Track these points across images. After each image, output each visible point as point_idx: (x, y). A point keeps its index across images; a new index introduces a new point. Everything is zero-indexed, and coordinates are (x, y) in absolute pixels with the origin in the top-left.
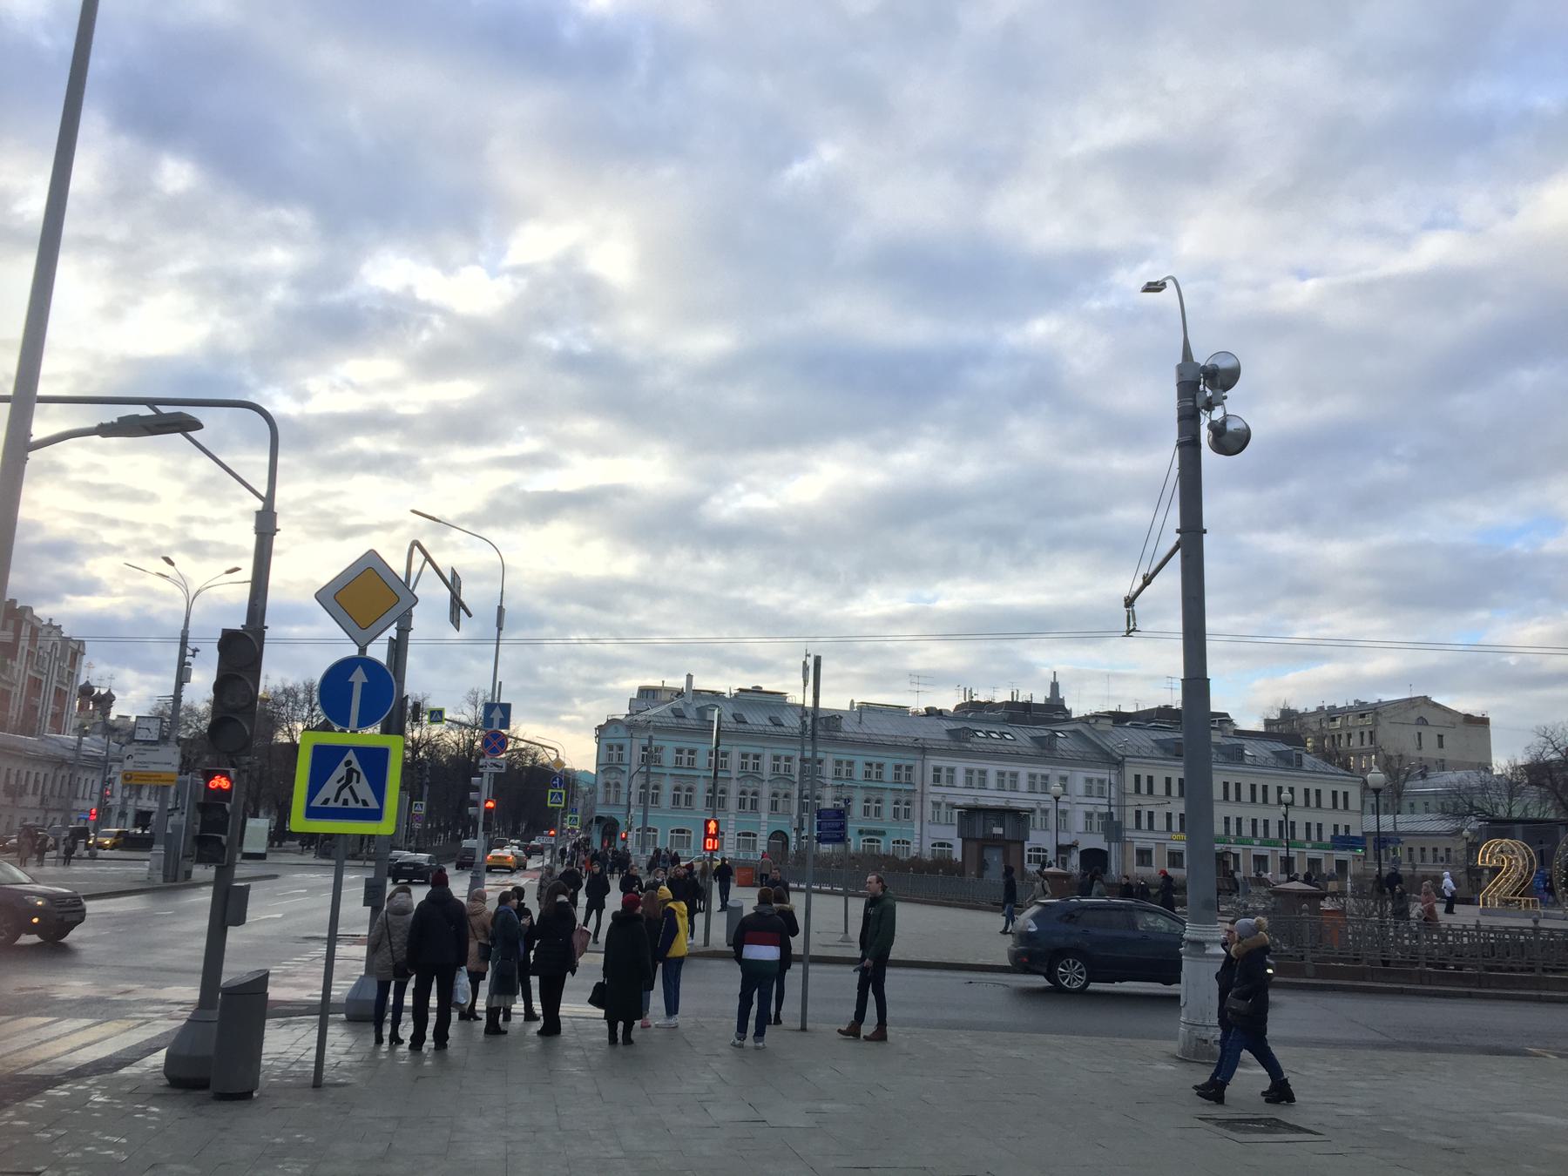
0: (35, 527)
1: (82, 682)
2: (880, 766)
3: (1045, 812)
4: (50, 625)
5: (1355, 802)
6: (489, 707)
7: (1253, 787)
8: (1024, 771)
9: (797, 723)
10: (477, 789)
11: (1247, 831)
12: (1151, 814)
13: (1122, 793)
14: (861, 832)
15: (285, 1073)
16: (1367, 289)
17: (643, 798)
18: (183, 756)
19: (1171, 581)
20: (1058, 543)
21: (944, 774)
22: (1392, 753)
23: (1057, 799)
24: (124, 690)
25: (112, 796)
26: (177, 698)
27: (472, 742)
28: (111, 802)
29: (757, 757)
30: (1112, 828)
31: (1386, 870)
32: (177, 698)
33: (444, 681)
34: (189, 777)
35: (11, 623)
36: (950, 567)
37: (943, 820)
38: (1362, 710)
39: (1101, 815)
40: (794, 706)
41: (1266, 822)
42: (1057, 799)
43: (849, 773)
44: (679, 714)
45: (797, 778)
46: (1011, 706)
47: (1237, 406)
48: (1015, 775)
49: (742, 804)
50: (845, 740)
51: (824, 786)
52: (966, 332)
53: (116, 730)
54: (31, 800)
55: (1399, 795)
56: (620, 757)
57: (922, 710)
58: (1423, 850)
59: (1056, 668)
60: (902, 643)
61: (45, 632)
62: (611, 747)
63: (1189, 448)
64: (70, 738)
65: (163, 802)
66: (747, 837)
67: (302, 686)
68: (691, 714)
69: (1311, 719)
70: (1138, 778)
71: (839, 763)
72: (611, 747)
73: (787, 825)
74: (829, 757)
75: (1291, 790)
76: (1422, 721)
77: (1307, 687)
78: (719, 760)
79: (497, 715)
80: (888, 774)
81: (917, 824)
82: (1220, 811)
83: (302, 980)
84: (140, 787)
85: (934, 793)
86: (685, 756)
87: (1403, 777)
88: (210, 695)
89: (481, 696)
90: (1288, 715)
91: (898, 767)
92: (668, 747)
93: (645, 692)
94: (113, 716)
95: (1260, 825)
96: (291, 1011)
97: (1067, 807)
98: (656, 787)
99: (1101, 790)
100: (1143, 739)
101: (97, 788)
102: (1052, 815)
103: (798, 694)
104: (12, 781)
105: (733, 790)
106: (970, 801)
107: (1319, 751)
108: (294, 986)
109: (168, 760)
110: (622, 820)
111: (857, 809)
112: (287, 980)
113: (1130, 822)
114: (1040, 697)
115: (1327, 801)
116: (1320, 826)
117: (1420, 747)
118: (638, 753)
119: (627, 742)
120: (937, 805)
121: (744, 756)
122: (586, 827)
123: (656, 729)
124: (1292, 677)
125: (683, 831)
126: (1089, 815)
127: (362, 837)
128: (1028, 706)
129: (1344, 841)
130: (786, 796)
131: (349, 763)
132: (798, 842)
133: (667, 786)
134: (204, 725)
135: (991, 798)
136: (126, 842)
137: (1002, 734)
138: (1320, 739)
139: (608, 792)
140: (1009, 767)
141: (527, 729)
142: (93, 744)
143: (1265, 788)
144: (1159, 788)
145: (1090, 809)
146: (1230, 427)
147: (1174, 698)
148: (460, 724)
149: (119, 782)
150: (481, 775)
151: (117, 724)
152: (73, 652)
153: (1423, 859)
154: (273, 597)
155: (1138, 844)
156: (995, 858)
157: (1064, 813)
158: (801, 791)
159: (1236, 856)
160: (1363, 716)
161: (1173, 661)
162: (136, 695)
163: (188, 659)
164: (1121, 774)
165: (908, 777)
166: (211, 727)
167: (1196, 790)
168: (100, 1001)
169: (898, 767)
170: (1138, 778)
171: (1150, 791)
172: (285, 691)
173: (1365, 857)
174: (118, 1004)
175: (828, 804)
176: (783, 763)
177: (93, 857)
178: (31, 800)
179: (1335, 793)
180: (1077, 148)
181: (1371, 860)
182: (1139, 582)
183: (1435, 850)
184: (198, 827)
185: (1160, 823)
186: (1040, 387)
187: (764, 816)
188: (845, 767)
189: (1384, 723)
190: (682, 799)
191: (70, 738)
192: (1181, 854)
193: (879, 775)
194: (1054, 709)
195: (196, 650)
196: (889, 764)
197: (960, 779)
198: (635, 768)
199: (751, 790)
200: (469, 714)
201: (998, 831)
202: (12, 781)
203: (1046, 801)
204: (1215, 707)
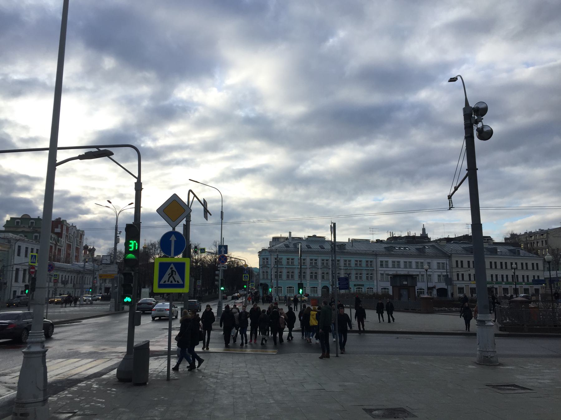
1: (84, 245)
2: (360, 261)
3: (423, 275)
4: (72, 226)
5: (541, 266)
6: (220, 247)
7: (501, 263)
8: (414, 261)
9: (330, 247)
10: (218, 275)
11: (500, 279)
12: (463, 275)
13: (451, 268)
14: (355, 285)
15: (158, 376)
16: (552, 69)
17: (276, 276)
18: (119, 268)
19: (465, 189)
20: (429, 176)
21: (384, 263)
22: (554, 248)
23: (427, 270)
24: (99, 246)
26: (115, 248)
27: (216, 259)
28: (96, 285)
29: (316, 260)
30: (448, 280)
31: (554, 291)
32: (115, 248)
33: (204, 238)
36: (389, 187)
37: (385, 280)
38: (542, 233)
39: (444, 276)
40: (328, 241)
41: (507, 276)
42: (427, 270)
43: (349, 264)
44: (287, 246)
45: (331, 267)
46: (408, 237)
47: (488, 122)
48: (410, 262)
49: (311, 277)
50: (347, 253)
51: (341, 269)
52: (397, 98)
53: (96, 260)
54: (70, 285)
56: (267, 262)
57: (375, 240)
59: (424, 223)
60: (368, 217)
62: (264, 259)
63: (469, 139)
65: (113, 285)
66: (314, 289)
67: (157, 243)
68: (291, 246)
69: (523, 237)
70: (457, 261)
71: (345, 261)
72: (264, 259)
73: (328, 284)
74: (342, 259)
75: (516, 264)
77: (521, 225)
78: (302, 262)
79: (223, 249)
80: (364, 264)
81: (375, 282)
82: (489, 273)
83: (162, 343)
84: (105, 280)
85: (381, 270)
86: (290, 261)
89: (218, 243)
90: (513, 236)
91: (367, 262)
92: (284, 258)
93: (275, 239)
94: (95, 256)
95: (505, 277)
96: (157, 354)
97: (431, 273)
98: (281, 272)
99: (443, 267)
100: (459, 247)
101: (91, 281)
102: (425, 276)
103: (329, 237)
104: (64, 279)
105: (308, 272)
106: (395, 273)
107: (526, 248)
108: (160, 345)
109: (113, 270)
110: (269, 284)
111: (353, 277)
112: (157, 344)
113: (455, 278)
114: (418, 233)
115: (530, 267)
116: (528, 276)
118: (273, 260)
119: (269, 257)
120: (382, 274)
121: (311, 260)
122: (257, 287)
123: (279, 252)
124: (519, 221)
125: (291, 287)
126: (439, 276)
127: (179, 293)
128: (414, 237)
129: (537, 281)
130: (327, 273)
131: (172, 268)
132: (332, 290)
133: (285, 272)
135: (402, 271)
136: (104, 299)
137: (405, 248)
138: (526, 244)
139: (264, 275)
140: (408, 260)
141: (234, 254)
142: (89, 266)
143: (506, 263)
144: (465, 265)
145: (440, 274)
146: (485, 130)
147: (469, 231)
148: (211, 253)
149: (98, 279)
150: (219, 270)
152: (80, 234)
155: (458, 286)
156: (404, 292)
157: (430, 275)
158: (332, 271)
159: (496, 289)
160: (542, 235)
161: (467, 217)
162: (102, 247)
164: (450, 261)
165: (371, 265)
167: (479, 266)
169: (367, 262)
170: (457, 261)
171: (462, 266)
172: (151, 244)
173: (546, 287)
175: (342, 276)
176: (325, 262)
177: (91, 304)
178: (70, 285)
179: (533, 264)
180: (437, 24)
181: (548, 288)
182: (453, 189)
185: (466, 277)
186: (424, 117)
187: (320, 281)
188: (348, 263)
190: (290, 276)
192: (475, 289)
193: (360, 265)
194: (424, 237)
195: (120, 232)
196: (364, 260)
197: (390, 265)
198: (273, 266)
199: (314, 272)
200: (214, 250)
201: (405, 283)
202: (64, 279)
203: (423, 271)
204: (485, 234)
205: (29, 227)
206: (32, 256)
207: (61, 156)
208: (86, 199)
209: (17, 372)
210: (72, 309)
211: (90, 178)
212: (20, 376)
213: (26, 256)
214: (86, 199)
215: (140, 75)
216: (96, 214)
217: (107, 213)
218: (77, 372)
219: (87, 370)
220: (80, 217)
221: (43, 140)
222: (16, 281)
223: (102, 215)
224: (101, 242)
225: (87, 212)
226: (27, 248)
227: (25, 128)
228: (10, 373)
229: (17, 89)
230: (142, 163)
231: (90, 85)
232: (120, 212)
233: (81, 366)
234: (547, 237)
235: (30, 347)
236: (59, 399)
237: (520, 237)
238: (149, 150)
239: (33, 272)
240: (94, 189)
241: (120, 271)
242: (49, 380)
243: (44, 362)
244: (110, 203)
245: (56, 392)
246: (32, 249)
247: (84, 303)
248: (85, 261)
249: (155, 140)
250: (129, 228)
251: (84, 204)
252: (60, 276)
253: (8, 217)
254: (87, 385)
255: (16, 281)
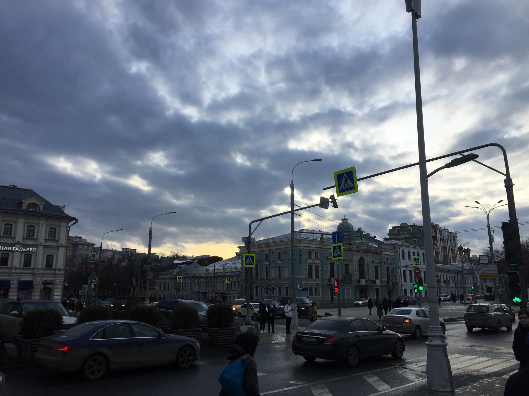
0: (436, 198)
4: (445, 229)
18: (498, 268)
25: (477, 282)
28: (478, 285)
34: (502, 275)
35: (433, 230)
61: (444, 231)
64: (459, 264)
65: (495, 284)
84: (486, 279)
88: (503, 245)
94: (471, 256)
101: (472, 280)
104: (445, 279)
109: (493, 269)
134: (503, 256)
142: (467, 266)
151: (473, 258)
152: (454, 236)
154: (516, 206)
162: (477, 248)
163: (492, 234)
166: (507, 256)
168: (490, 352)
174: (496, 353)
178: (452, 285)
184: (510, 292)
191: (459, 264)
195: (494, 231)
202: (445, 279)
205: (408, 234)
206: (415, 258)
207: (430, 167)
208: (455, 201)
209: (423, 361)
210: (458, 307)
211: (456, 181)
212: (428, 365)
213: (410, 259)
214: (455, 201)
215: (493, 64)
216: (467, 215)
217: (478, 213)
218: (476, 369)
219: (485, 368)
220: (452, 220)
221: (410, 153)
222: (405, 281)
223: (471, 216)
224: (476, 242)
225: (458, 214)
226: (409, 252)
227: (393, 147)
228: (415, 362)
229: (381, 116)
230: (508, 156)
231: (444, 92)
232: (490, 211)
233: (479, 363)
235: (431, 341)
236: (464, 392)
238: (515, 139)
239: (418, 273)
240: (461, 190)
241: (500, 271)
242: (453, 373)
243: (446, 356)
244: (478, 203)
245: (459, 386)
246: (414, 253)
247: (469, 302)
248: (462, 261)
249: (519, 127)
250: (505, 226)
251: (453, 206)
252: (442, 277)
253: (390, 227)
254: (489, 383)
255: (405, 281)
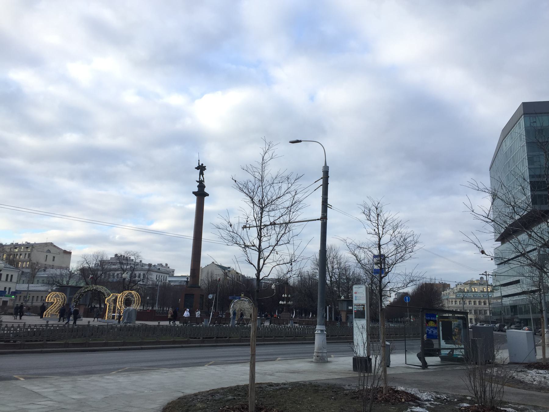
55: (34, 277)
58: (38, 297)
69: (7, 247)
76: (49, 251)
87: (36, 271)
117: (46, 260)
138: (9, 255)
153: (37, 300)
183: (42, 297)
189: (35, 251)
234: (32, 250)
237: (5, 247)
